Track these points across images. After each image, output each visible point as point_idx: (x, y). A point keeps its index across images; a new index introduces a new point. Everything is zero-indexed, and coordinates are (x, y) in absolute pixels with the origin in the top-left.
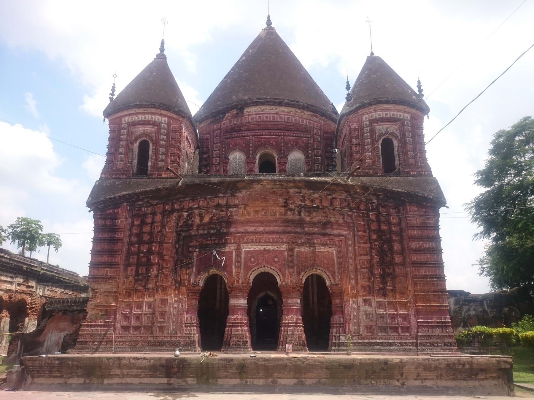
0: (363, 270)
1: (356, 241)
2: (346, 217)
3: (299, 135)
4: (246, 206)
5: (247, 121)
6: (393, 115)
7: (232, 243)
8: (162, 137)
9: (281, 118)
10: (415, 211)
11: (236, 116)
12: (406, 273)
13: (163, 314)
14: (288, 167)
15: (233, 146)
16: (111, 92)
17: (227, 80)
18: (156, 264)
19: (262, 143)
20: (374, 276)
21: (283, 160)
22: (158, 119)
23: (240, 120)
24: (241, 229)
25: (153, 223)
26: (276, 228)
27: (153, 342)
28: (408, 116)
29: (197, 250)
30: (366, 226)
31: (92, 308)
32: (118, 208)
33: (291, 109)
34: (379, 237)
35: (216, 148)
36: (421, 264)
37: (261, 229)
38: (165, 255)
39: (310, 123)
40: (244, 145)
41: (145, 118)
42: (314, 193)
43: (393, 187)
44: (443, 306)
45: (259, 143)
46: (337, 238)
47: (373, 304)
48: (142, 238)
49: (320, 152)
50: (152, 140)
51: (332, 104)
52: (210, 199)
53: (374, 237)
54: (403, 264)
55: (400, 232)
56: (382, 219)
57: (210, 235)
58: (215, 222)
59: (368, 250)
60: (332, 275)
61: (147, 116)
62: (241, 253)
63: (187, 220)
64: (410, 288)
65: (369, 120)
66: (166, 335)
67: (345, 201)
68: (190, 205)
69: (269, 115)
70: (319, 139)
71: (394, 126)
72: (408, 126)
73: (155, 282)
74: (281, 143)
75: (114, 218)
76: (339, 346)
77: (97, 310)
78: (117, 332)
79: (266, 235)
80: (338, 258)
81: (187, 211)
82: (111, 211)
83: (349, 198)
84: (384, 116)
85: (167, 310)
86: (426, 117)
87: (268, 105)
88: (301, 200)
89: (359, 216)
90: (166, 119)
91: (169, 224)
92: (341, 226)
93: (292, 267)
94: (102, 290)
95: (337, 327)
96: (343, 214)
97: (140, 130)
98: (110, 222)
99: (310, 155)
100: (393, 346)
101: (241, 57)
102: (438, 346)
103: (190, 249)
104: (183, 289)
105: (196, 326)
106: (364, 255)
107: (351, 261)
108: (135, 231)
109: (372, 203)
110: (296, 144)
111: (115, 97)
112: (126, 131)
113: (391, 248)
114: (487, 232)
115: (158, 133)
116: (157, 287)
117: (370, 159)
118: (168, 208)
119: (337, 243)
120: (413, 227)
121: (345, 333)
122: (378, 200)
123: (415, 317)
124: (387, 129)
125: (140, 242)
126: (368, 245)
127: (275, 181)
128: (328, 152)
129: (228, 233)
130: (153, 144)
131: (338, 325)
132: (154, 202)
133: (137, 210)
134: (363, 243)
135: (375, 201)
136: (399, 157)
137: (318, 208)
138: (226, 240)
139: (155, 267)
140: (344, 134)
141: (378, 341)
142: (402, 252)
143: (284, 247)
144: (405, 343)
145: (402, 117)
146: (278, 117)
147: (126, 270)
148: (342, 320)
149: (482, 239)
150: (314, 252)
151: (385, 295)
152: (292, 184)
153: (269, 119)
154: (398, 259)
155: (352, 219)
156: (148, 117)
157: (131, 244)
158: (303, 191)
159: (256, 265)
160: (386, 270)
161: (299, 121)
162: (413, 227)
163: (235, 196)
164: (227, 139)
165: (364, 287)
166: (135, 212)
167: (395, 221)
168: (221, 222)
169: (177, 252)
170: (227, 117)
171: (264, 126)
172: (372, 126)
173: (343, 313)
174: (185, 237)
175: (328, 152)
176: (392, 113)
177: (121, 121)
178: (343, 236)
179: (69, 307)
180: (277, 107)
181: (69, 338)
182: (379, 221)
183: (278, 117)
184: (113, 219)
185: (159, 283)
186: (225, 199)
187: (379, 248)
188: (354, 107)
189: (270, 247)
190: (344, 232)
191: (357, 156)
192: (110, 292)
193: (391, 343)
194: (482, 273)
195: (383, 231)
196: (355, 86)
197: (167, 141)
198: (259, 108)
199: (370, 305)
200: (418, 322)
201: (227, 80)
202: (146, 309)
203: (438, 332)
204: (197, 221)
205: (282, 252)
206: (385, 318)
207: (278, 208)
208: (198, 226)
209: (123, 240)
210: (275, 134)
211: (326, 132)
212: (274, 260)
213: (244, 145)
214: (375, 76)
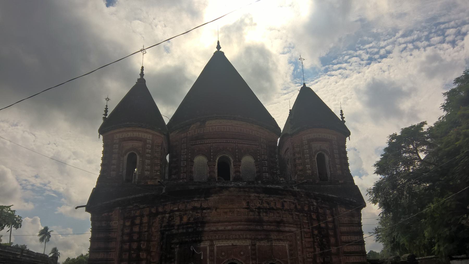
0: (309, 260)
4: (216, 209)
7: (206, 240)
8: (148, 151)
16: (104, 113)
25: (141, 223)
26: (241, 227)
29: (178, 246)
37: (229, 228)
38: (152, 252)
42: (270, 197)
46: (288, 234)
52: (188, 202)
53: (316, 232)
56: (321, 218)
67: (293, 203)
80: (290, 250)
81: (169, 213)
82: (106, 214)
83: (296, 201)
86: (347, 138)
88: (259, 203)
90: (151, 136)
92: (291, 224)
96: (292, 214)
106: (309, 248)
107: (299, 253)
108: (126, 231)
109: (313, 205)
111: (107, 117)
112: (117, 145)
117: (310, 170)
118: (153, 210)
122: (317, 203)
125: (131, 240)
126: (312, 239)
127: (240, 188)
132: (141, 206)
134: (307, 238)
135: (315, 204)
136: (330, 169)
137: (273, 209)
143: (248, 243)
154: (333, 250)
156: (136, 134)
158: (262, 195)
163: (207, 200)
167: (330, 219)
178: (292, 232)
182: (318, 220)
189: (236, 243)
190: (294, 229)
204: (177, 221)
205: (246, 247)
207: (242, 210)
208: (179, 226)
213: (206, 151)
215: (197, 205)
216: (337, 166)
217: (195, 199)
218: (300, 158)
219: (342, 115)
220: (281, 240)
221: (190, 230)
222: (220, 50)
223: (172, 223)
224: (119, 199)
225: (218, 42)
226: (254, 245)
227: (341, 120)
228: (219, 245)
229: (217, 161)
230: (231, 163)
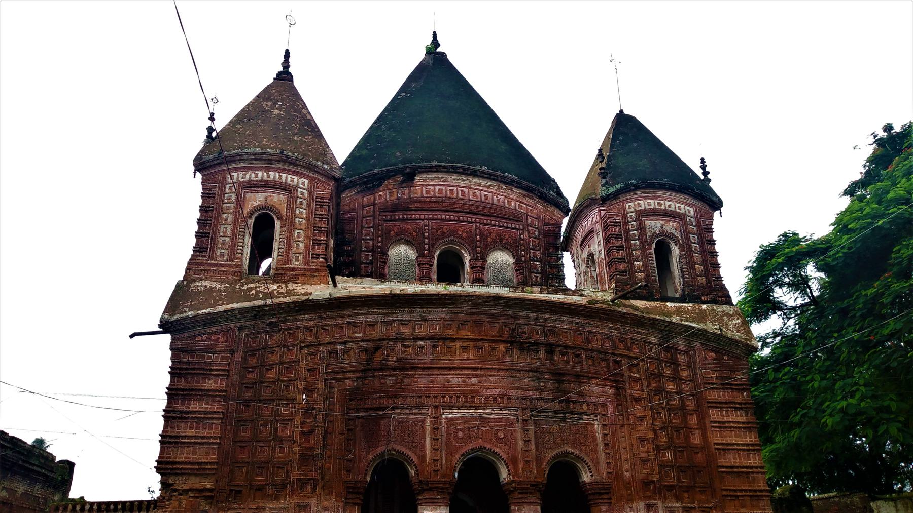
4: (445, 339)
6: (670, 206)
14: (486, 276)
15: (396, 234)
17: (379, 127)
21: (479, 264)
22: (292, 180)
23: (407, 192)
28: (692, 210)
35: (367, 235)
39: (521, 207)
40: (414, 234)
41: (269, 176)
43: (681, 320)
45: (439, 233)
49: (538, 254)
51: (554, 181)
61: (272, 174)
65: (636, 211)
67: (609, 339)
70: (537, 234)
74: (477, 235)
86: (716, 214)
87: (456, 173)
90: (306, 181)
99: (523, 259)
117: (641, 271)
124: (662, 227)
126: (648, 414)
128: (550, 255)
136: (682, 272)
140: (586, 229)
145: (682, 211)
164: (385, 221)
170: (387, 186)
171: (446, 205)
172: (640, 220)
175: (550, 255)
177: (224, 178)
201: (379, 127)
205: (510, 423)
210: (465, 219)
211: (547, 224)
212: (496, 434)
215: (406, 330)
216: (697, 266)
218: (620, 248)
219: (703, 167)
222: (439, 50)
224: (236, 306)
225: (435, 35)
227: (702, 177)
230: (463, 265)
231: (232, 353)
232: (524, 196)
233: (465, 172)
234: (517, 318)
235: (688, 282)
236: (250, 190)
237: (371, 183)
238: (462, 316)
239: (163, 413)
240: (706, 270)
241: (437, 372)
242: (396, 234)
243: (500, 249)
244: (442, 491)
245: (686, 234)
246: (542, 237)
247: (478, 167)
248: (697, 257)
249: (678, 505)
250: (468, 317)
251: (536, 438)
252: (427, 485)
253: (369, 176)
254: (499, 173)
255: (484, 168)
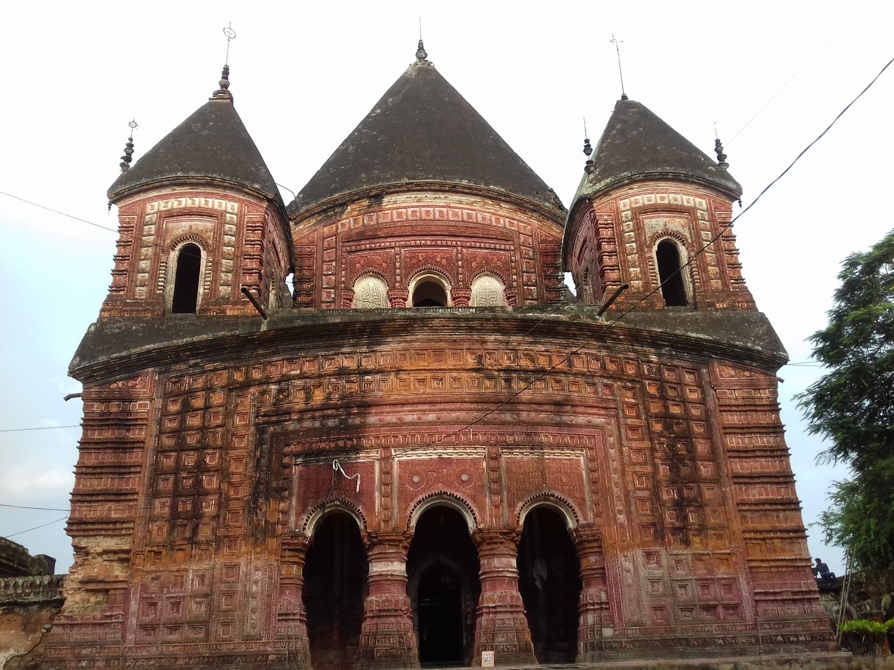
1: (624, 437)
2: (600, 389)
3: (492, 246)
4: (398, 371)
5: (389, 220)
6: (676, 200)
7: (372, 447)
8: (227, 238)
9: (456, 214)
10: (732, 376)
11: (368, 210)
12: (724, 498)
13: (230, 595)
15: (363, 266)
16: (125, 154)
17: (347, 149)
18: (214, 492)
19: (420, 261)
20: (663, 504)
22: (220, 206)
23: (375, 217)
24: (391, 418)
25: (207, 407)
26: (462, 415)
27: (208, 657)
30: (641, 407)
31: (75, 589)
32: (133, 378)
33: (472, 199)
34: (667, 427)
36: (751, 477)
37: (431, 417)
39: (511, 224)
40: (384, 265)
41: (193, 204)
42: (535, 343)
43: (687, 331)
44: (802, 560)
45: (414, 261)
46: (584, 431)
47: (664, 561)
48: (184, 438)
50: (206, 246)
51: (552, 191)
53: (658, 427)
54: (716, 480)
55: (706, 419)
56: (671, 393)
57: (325, 431)
58: (336, 404)
59: (648, 453)
60: (579, 505)
61: (197, 199)
62: (392, 466)
63: (278, 400)
64: (736, 526)
65: (632, 209)
66: (236, 641)
67: (597, 358)
68: (285, 370)
69: (431, 209)
70: (531, 254)
71: (677, 220)
72: (704, 220)
73: (213, 529)
74: (458, 260)
75: (127, 398)
76: (601, 649)
77: (88, 591)
78: (130, 637)
79: (441, 428)
80: (591, 470)
81: (278, 382)
82: (120, 384)
83: (604, 353)
84: (659, 201)
85: (240, 587)
86: (736, 203)
88: (509, 359)
89: (625, 387)
90: (236, 205)
91: (239, 409)
93: (498, 493)
94: (99, 550)
95: (594, 610)
96: (594, 384)
97: (182, 226)
98: (119, 406)
99: (515, 284)
100: (710, 645)
101: (373, 111)
102: (798, 642)
103: (286, 460)
104: (273, 543)
105: (301, 621)
107: (615, 477)
108: (169, 425)
110: (487, 263)
111: (132, 165)
112: (153, 227)
113: (691, 449)
114: (842, 448)
115: (219, 232)
116: (218, 540)
117: (638, 279)
118: (238, 377)
119: (585, 440)
120: (727, 408)
121: (613, 623)
122: (659, 355)
123: (748, 583)
126: (647, 444)
127: (457, 319)
129: (363, 425)
130: (209, 252)
131: (596, 607)
133: (174, 383)
135: (654, 358)
136: (692, 276)
138: (359, 438)
139: (213, 500)
140: (582, 240)
141: (679, 635)
142: (713, 456)
144: (734, 638)
146: (450, 212)
147: (150, 505)
148: (603, 596)
149: (833, 461)
150: (541, 460)
151: (686, 543)
152: (490, 325)
153: (432, 217)
154: (706, 470)
155: (612, 394)
156: (200, 202)
157: (161, 451)
159: (424, 490)
160: (685, 492)
161: (491, 220)
162: (727, 408)
164: (349, 252)
165: (645, 526)
166: (170, 387)
167: (694, 396)
168: (348, 406)
169: (257, 466)
170: (351, 212)
172: (637, 219)
173: (605, 583)
174: (274, 435)
175: (548, 277)
176: (672, 196)
178: (596, 426)
179: (19, 596)
180: (446, 195)
181: (16, 664)
182: (663, 397)
183: (450, 212)
184: (123, 400)
185: (221, 532)
186: (355, 356)
187: (667, 450)
188: (603, 183)
189: (450, 453)
191: (614, 275)
192: (115, 552)
193: (705, 640)
194: (831, 539)
195: (674, 417)
196: (600, 149)
197: (237, 245)
198: (413, 195)
199: (658, 562)
200: (756, 594)
201: (347, 149)
202: (191, 583)
203: (795, 610)
204: (298, 400)
205: (475, 462)
206: (689, 589)
207: (465, 375)
208: (301, 412)
209: (144, 442)
210: (444, 243)
211: (543, 241)
212: (460, 477)
214: (635, 133)
215: (349, 363)
217: (344, 350)
218: (611, 254)
220: (567, 446)
221: (331, 423)
223: (286, 406)
224: (152, 346)
226: (496, 458)
227: (717, 162)
228: (405, 458)
229: (411, 288)
231: (152, 400)
232: (515, 211)
233: (441, 189)
234: (484, 342)
235: (699, 288)
236: (172, 219)
237: (331, 211)
238: (417, 345)
239: (75, 470)
240: (722, 272)
241: (388, 409)
242: (363, 266)
243: (487, 275)
244: (393, 543)
245: (696, 233)
246: (537, 257)
247: (457, 181)
248: (710, 257)
249: (685, 552)
250: (425, 345)
251: (509, 479)
252: (377, 537)
253: (329, 203)
254: (483, 186)
255: (465, 182)
